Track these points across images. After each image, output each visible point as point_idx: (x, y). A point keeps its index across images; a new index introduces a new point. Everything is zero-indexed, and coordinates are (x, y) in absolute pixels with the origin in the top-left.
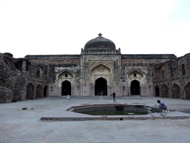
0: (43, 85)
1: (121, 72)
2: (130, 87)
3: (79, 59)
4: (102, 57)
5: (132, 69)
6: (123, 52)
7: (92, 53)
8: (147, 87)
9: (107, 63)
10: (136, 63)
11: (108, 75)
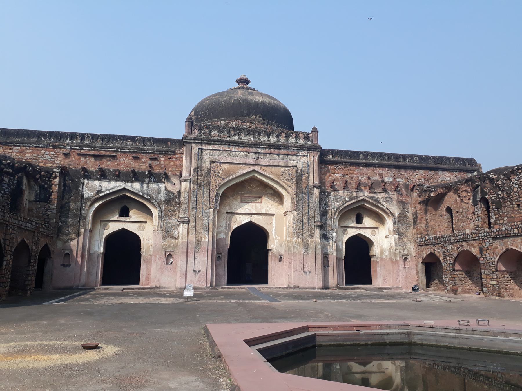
0: (36, 243)
1: (320, 208)
3: (177, 156)
4: (259, 153)
5: (351, 199)
6: (325, 144)
8: (398, 258)
9: (274, 174)
10: (363, 179)
11: (274, 215)
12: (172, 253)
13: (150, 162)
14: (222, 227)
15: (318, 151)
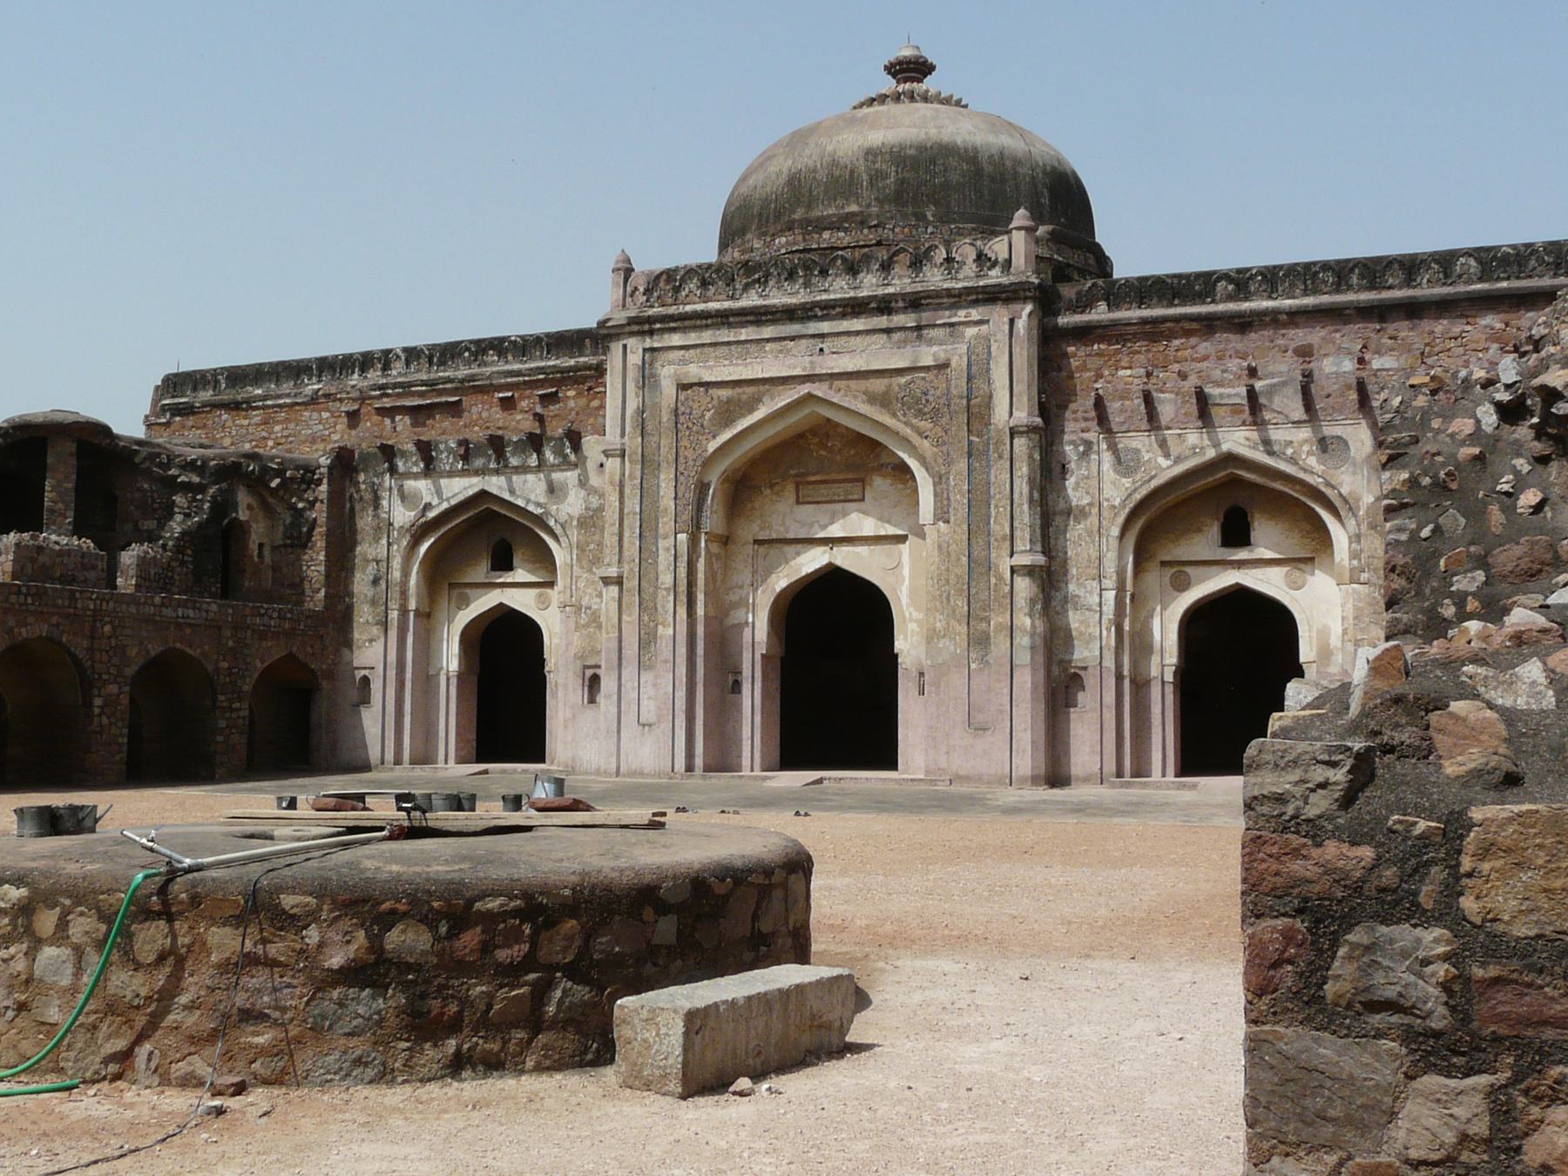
2: (1169, 677)
4: (822, 336)
7: (713, 306)
9: (872, 399)
12: (597, 671)
13: (539, 409)
14: (741, 587)
15: (1025, 300)
